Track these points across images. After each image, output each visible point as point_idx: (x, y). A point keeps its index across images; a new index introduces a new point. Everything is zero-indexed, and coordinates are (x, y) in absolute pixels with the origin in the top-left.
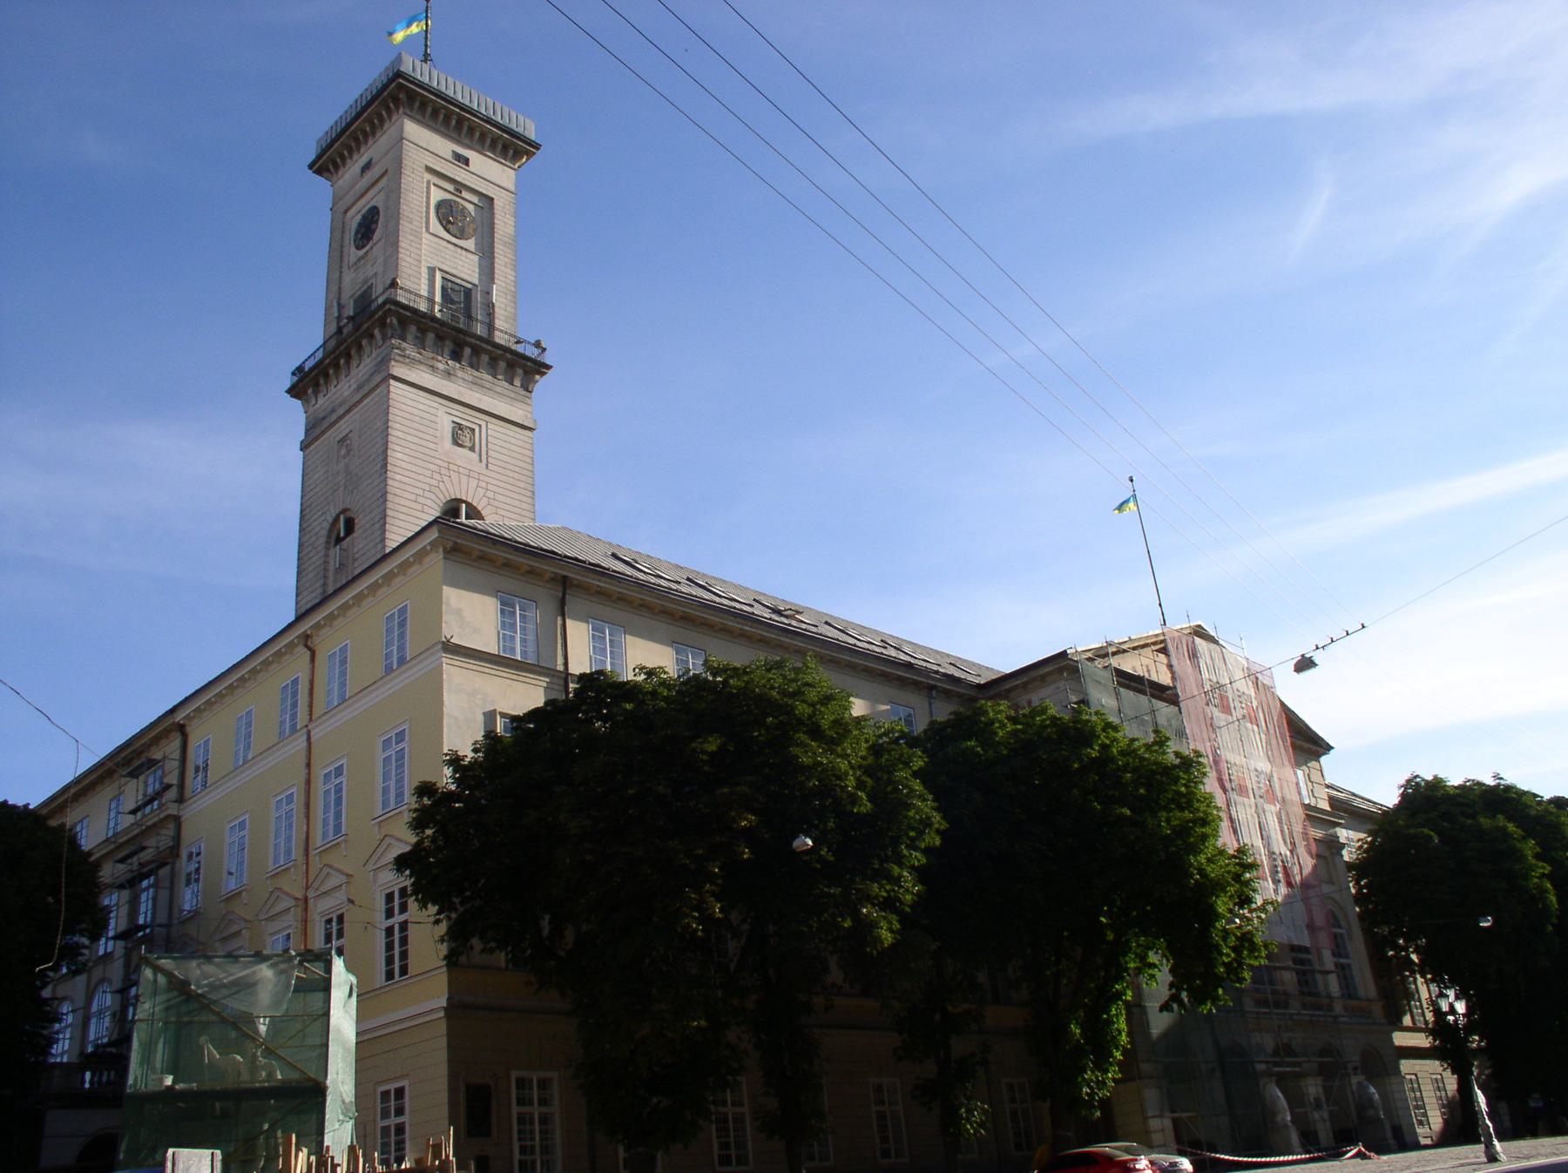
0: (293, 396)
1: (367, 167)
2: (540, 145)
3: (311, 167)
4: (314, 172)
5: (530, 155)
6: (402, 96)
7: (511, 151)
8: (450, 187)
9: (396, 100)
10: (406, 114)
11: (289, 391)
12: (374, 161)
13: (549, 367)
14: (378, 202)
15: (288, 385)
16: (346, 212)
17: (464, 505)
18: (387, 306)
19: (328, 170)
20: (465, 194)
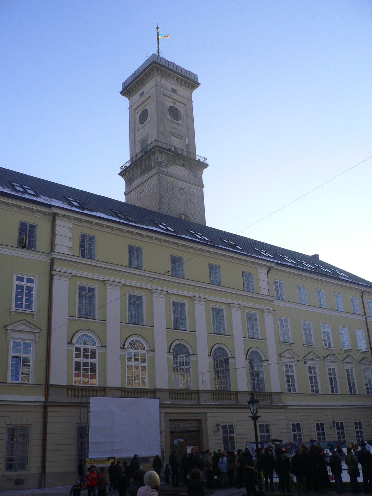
0: (120, 176)
1: (142, 95)
2: (199, 84)
3: (121, 93)
5: (197, 87)
7: (191, 86)
8: (172, 101)
11: (119, 174)
12: (145, 93)
14: (147, 107)
20: (177, 103)
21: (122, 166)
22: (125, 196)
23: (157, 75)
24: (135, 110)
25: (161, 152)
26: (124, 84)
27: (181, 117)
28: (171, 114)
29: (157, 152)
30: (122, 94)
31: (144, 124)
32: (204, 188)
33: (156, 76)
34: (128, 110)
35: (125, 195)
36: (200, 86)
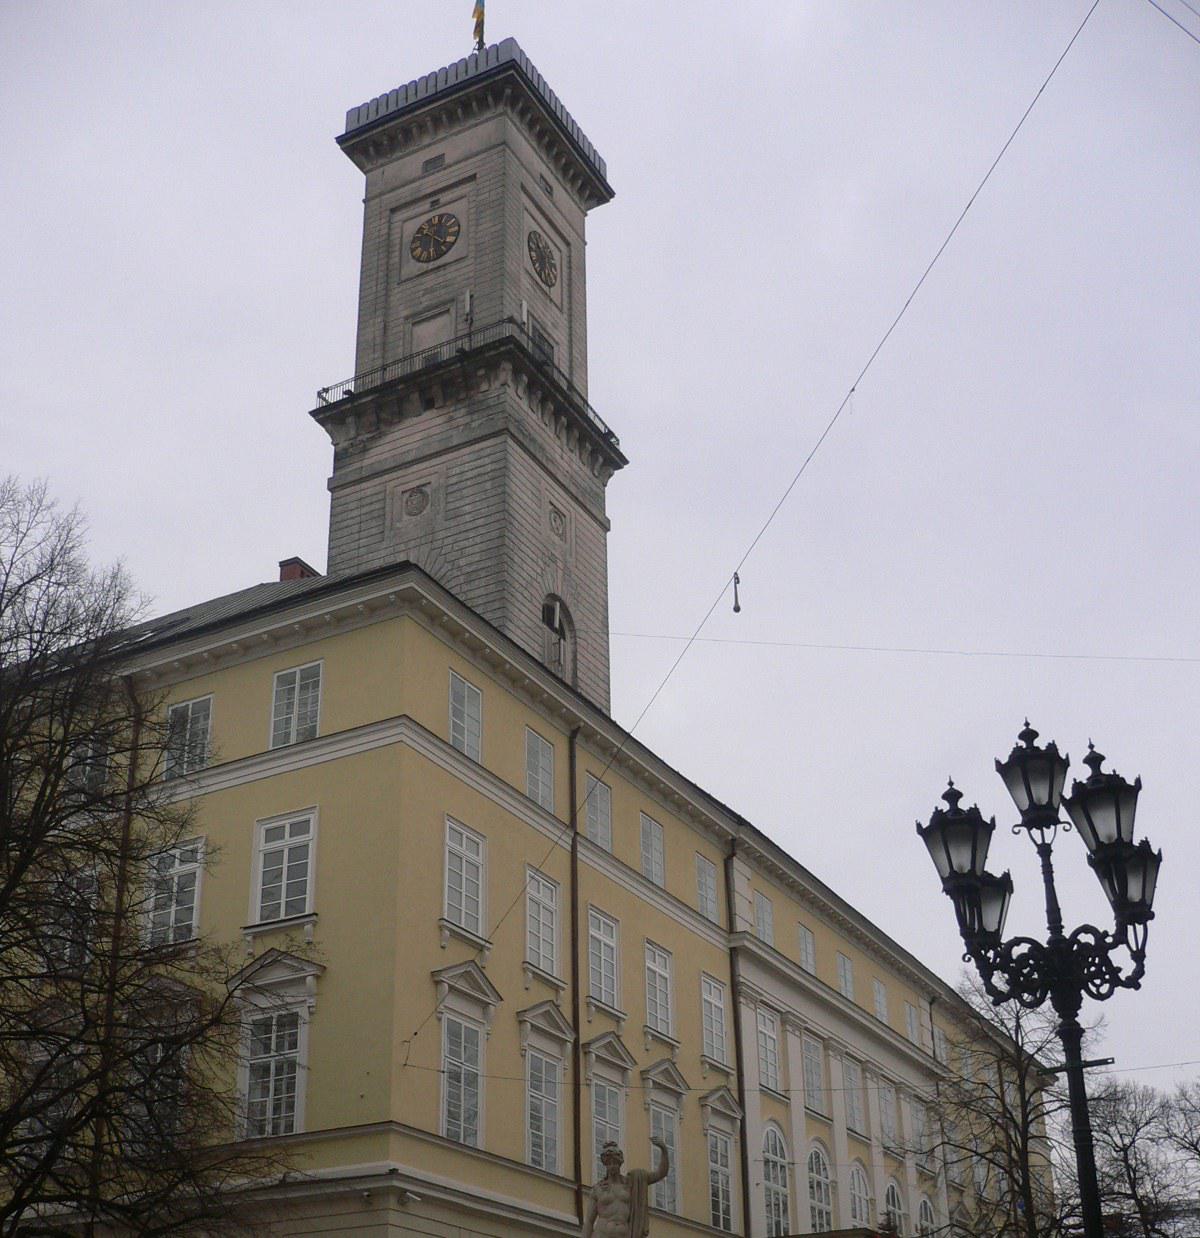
0: (317, 421)
1: (435, 164)
2: (612, 194)
3: (340, 140)
4: (343, 149)
6: (508, 91)
7: (588, 192)
9: (498, 97)
10: (504, 113)
11: (313, 413)
12: (448, 160)
13: (626, 462)
15: (314, 408)
16: (393, 211)
17: (558, 604)
18: (512, 346)
19: (365, 152)
21: (326, 390)
22: (330, 494)
23: (509, 111)
24: (393, 211)
25: (516, 373)
26: (354, 114)
27: (555, 278)
28: (533, 254)
29: (508, 366)
30: (344, 146)
31: (431, 265)
32: (608, 533)
33: (508, 116)
34: (363, 205)
35: (329, 489)
36: (612, 200)
